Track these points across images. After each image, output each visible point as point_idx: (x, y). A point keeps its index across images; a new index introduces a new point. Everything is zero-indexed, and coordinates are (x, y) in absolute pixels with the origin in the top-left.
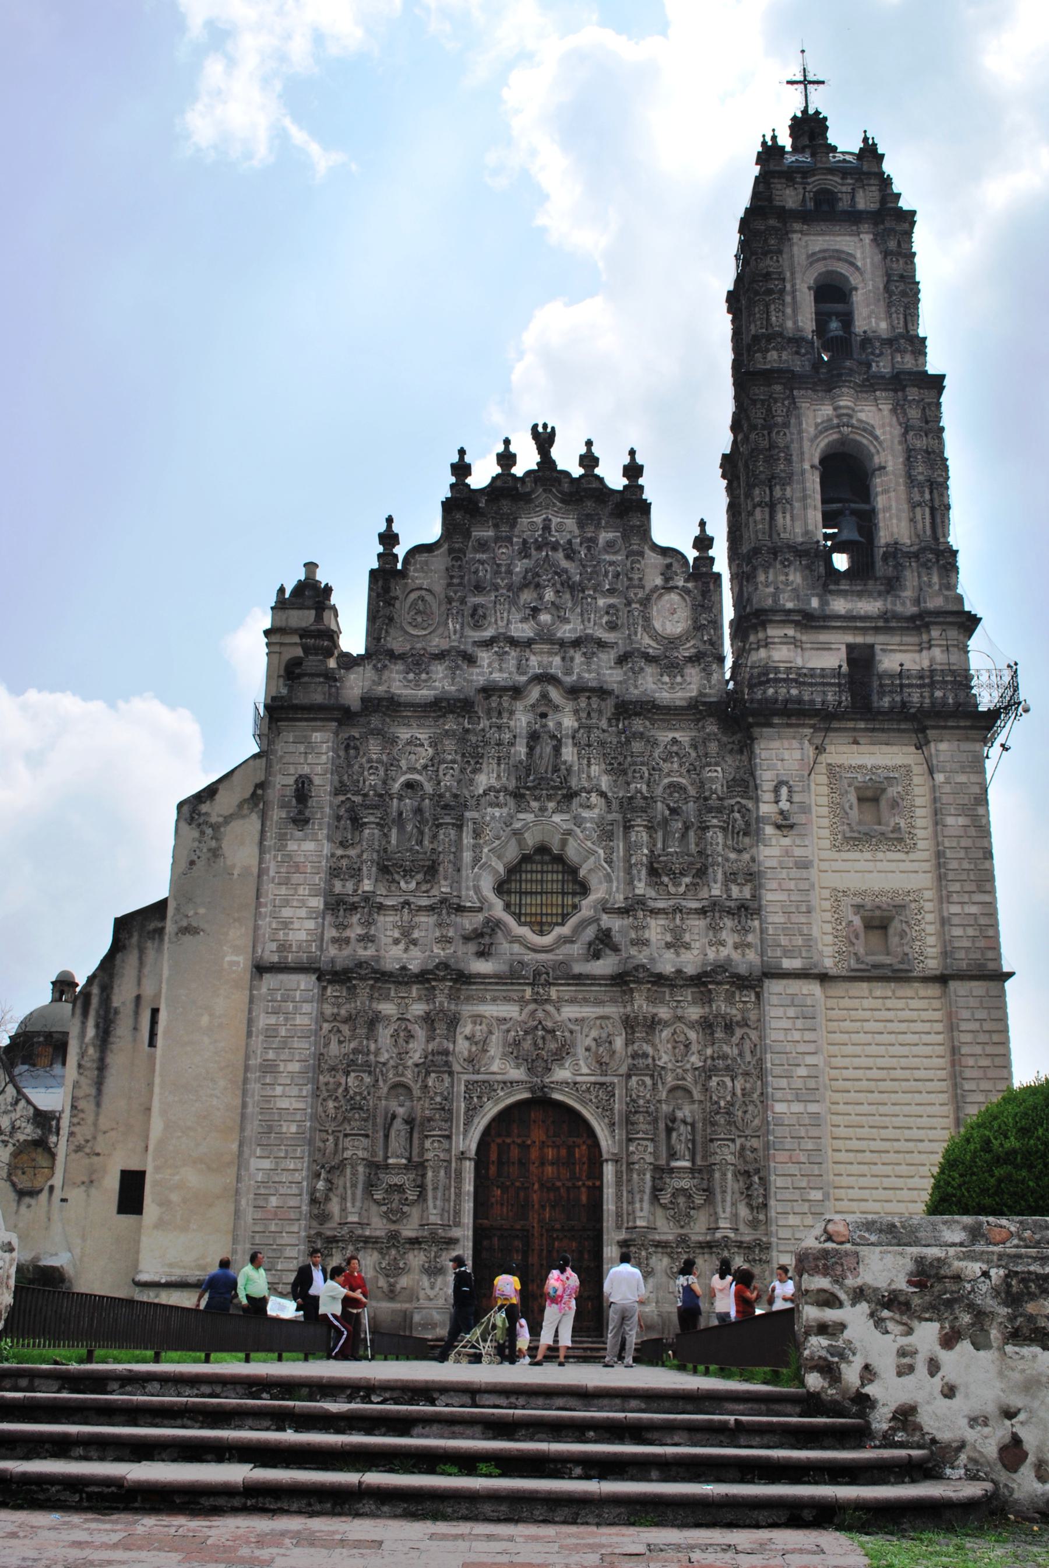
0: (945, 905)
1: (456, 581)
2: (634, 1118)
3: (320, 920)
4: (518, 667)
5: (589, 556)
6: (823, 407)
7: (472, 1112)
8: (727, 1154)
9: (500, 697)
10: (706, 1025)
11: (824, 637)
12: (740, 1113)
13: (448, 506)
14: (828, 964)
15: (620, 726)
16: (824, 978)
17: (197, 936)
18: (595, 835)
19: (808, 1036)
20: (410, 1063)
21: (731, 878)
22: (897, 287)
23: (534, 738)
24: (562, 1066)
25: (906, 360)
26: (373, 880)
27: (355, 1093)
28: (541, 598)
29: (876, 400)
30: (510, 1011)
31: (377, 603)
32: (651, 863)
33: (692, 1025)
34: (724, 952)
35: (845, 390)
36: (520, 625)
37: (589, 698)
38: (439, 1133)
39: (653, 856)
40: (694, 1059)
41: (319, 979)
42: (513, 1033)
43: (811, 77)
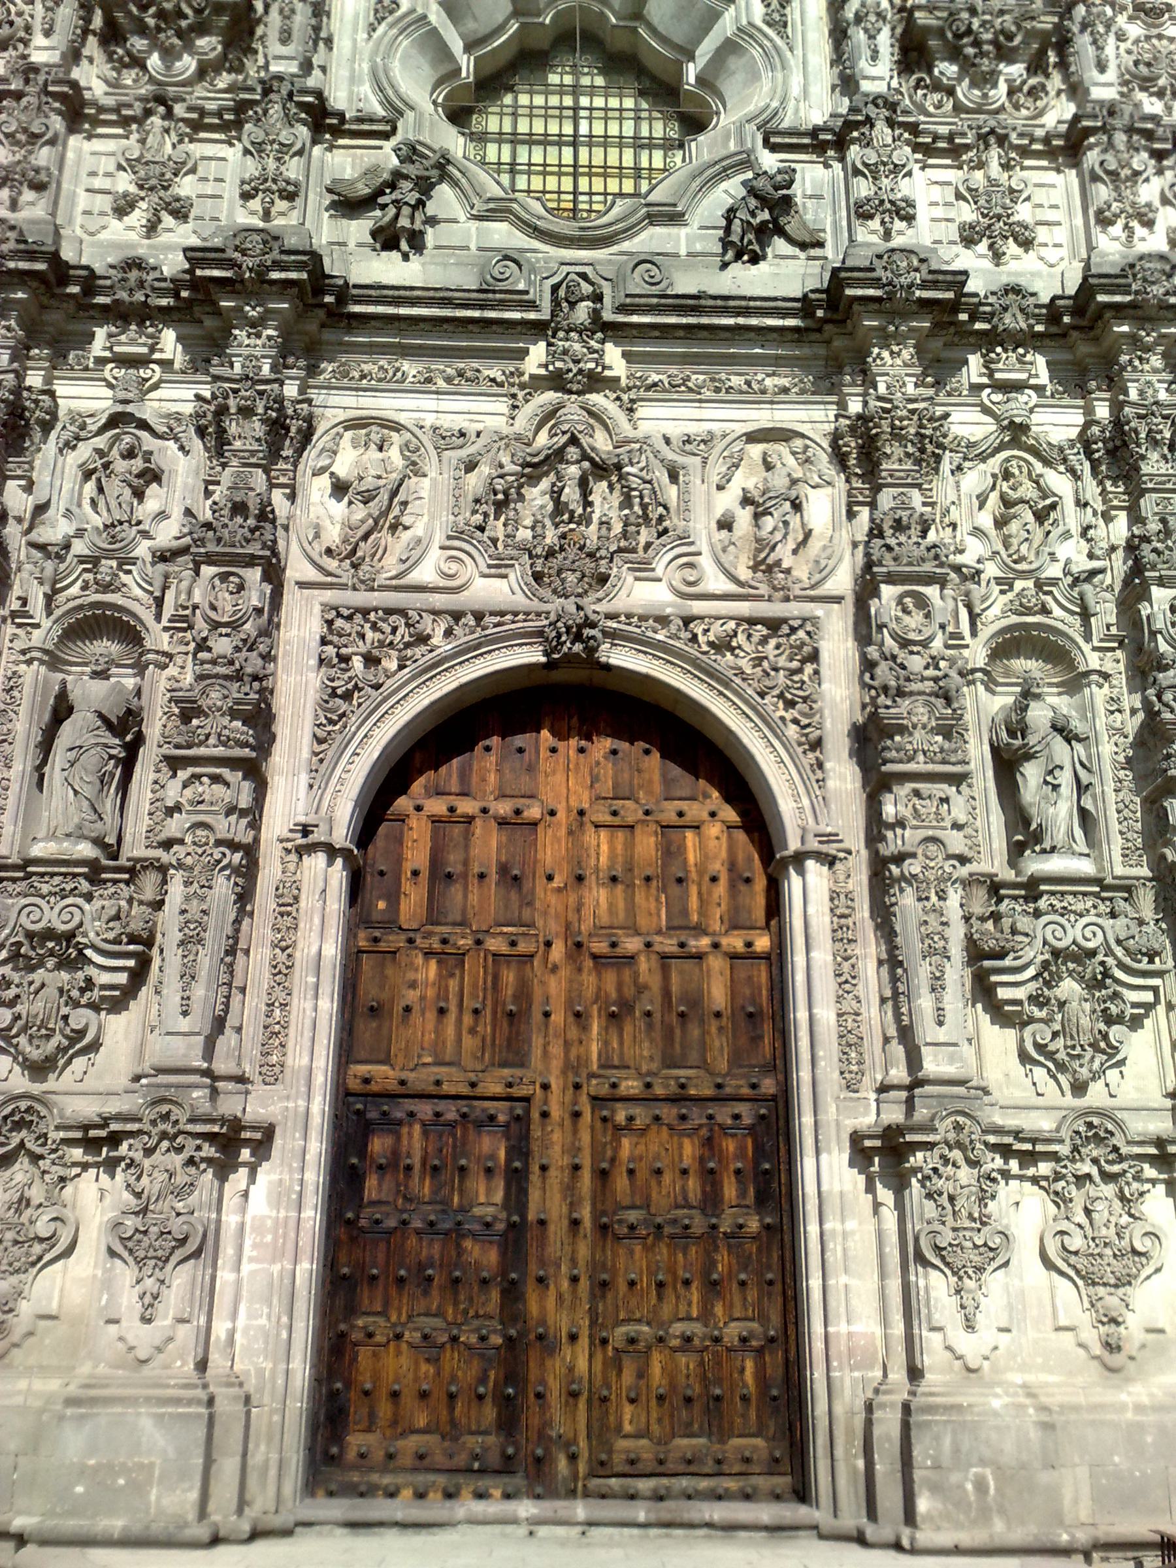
20: (143, 549)
24: (643, 569)
38: (220, 751)
42: (485, 469)
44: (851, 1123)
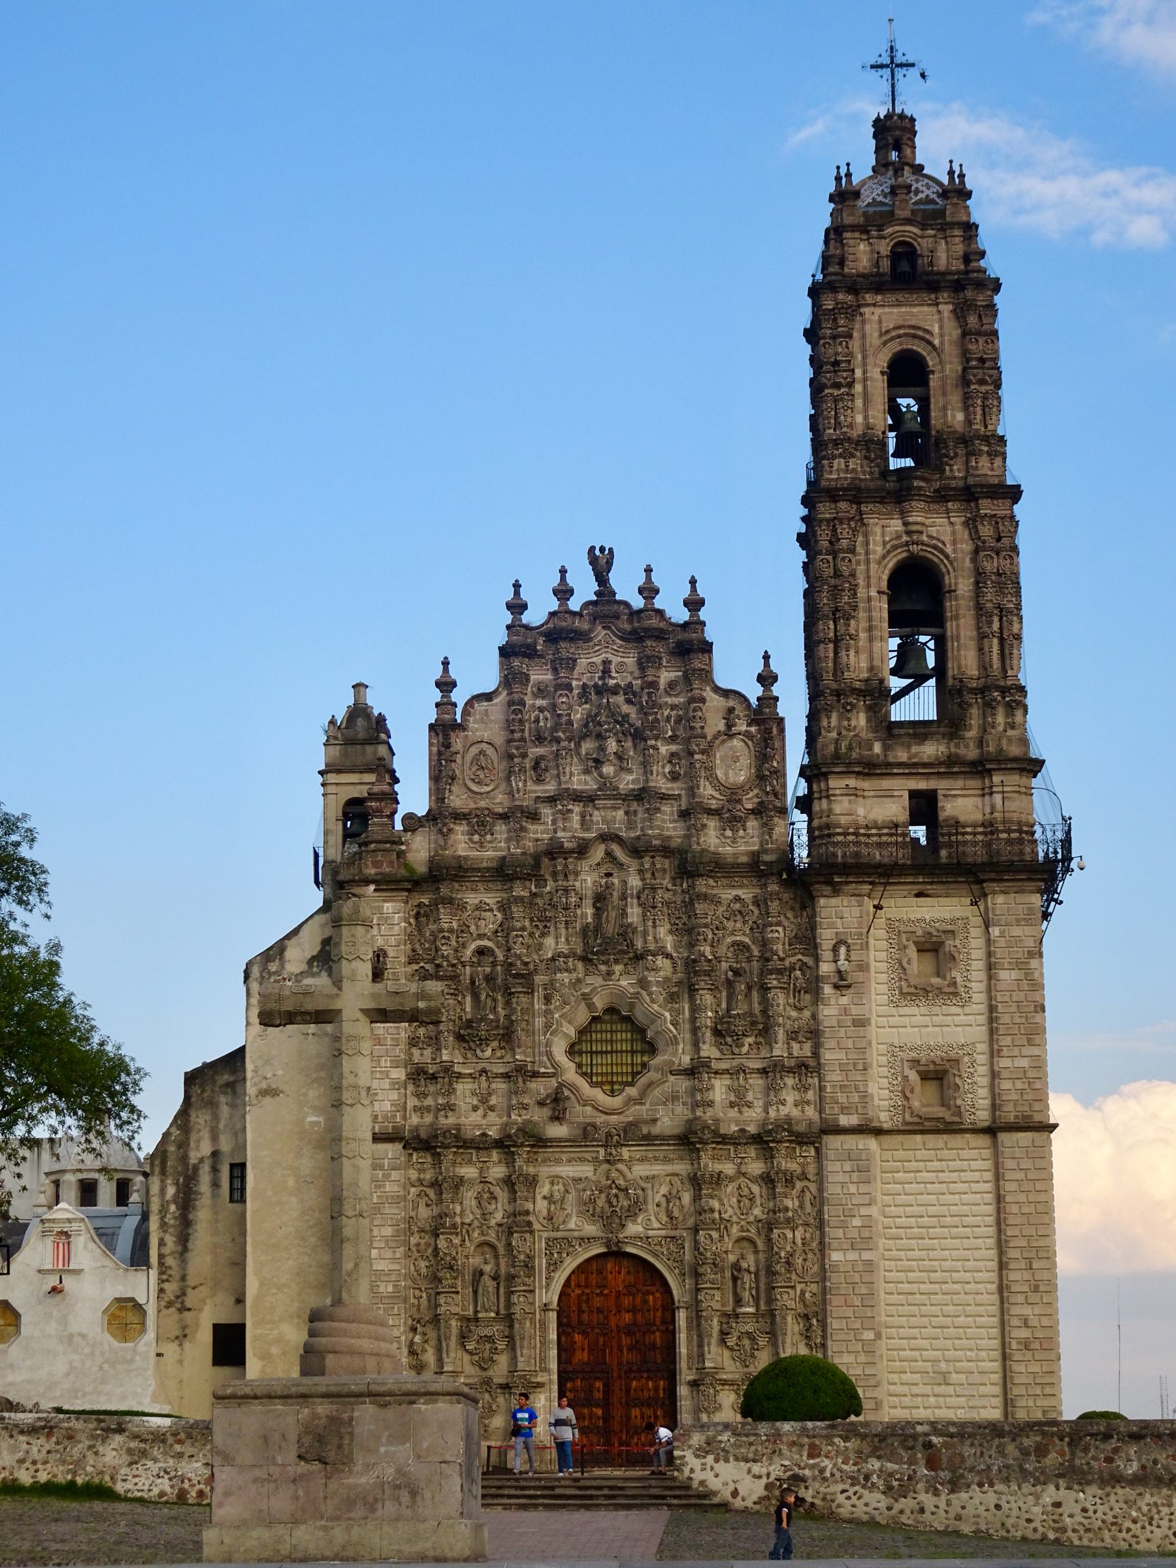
0: (995, 1059)
1: (517, 735)
2: (701, 1270)
3: (402, 1091)
4: (583, 822)
5: (650, 703)
6: (892, 522)
7: (553, 1266)
8: (787, 1300)
9: (566, 859)
10: (768, 1180)
11: (886, 783)
12: (800, 1261)
13: (505, 652)
14: (884, 1116)
15: (685, 885)
16: (878, 1132)
17: (277, 1098)
18: (661, 998)
19: (863, 1188)
20: (493, 1222)
21: (793, 1035)
22: (974, 376)
23: (600, 900)
25: (980, 464)
26: (450, 1049)
27: (445, 1254)
28: (602, 749)
29: (948, 511)
30: (585, 1170)
31: (439, 760)
32: (716, 1024)
33: (754, 1180)
34: (784, 1110)
35: (914, 503)
36: (583, 777)
37: (653, 857)
39: (718, 1020)
40: (757, 1211)
41: (404, 1147)
43: (899, 59)
44: (690, 1378)
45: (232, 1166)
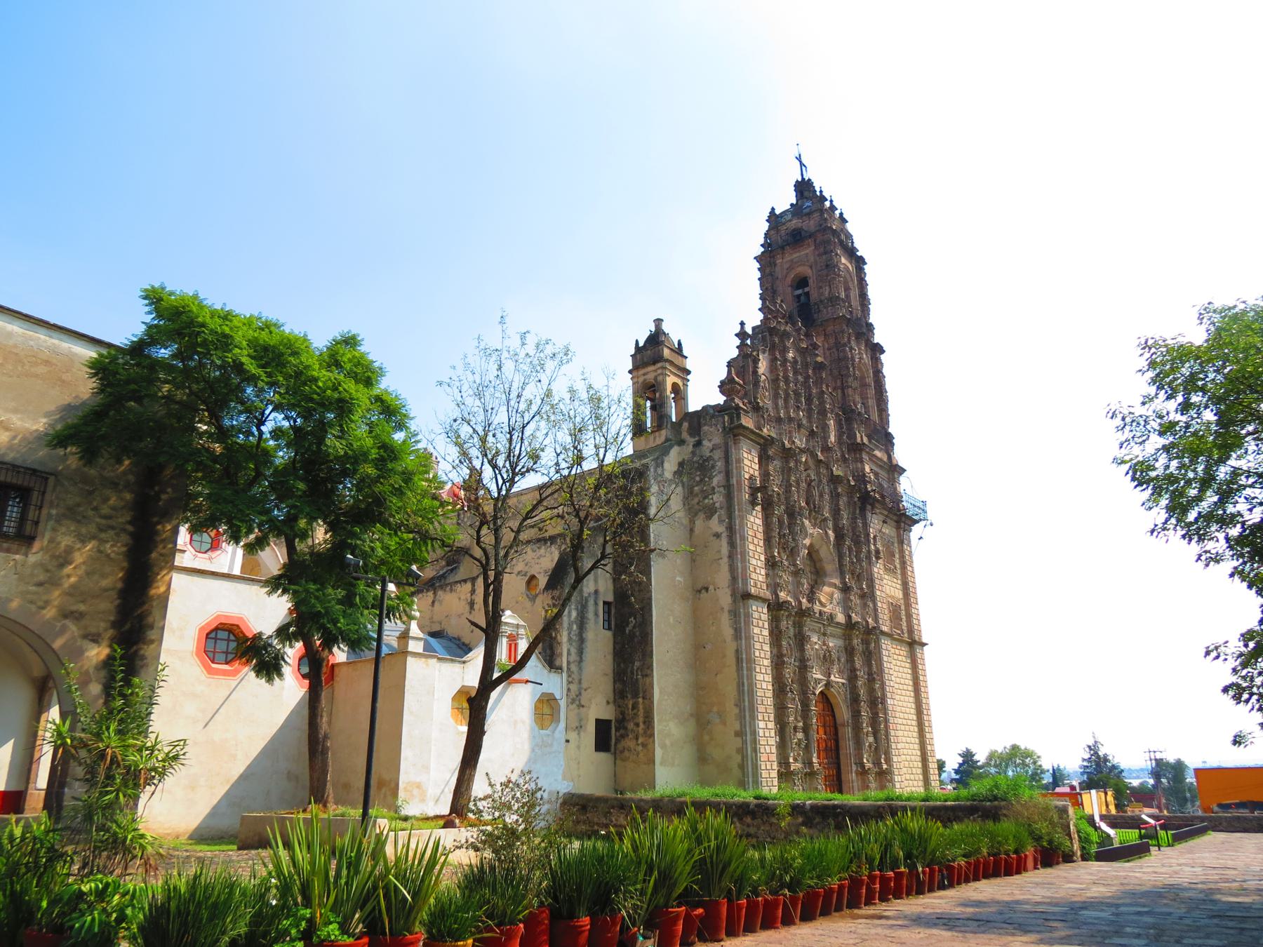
45: (605, 603)
